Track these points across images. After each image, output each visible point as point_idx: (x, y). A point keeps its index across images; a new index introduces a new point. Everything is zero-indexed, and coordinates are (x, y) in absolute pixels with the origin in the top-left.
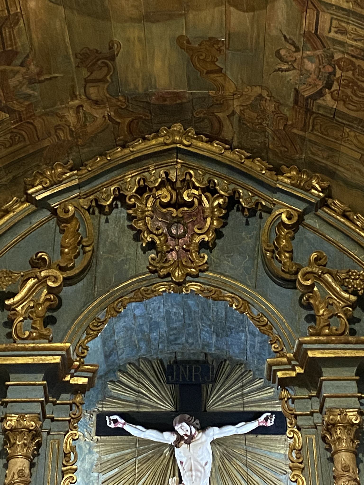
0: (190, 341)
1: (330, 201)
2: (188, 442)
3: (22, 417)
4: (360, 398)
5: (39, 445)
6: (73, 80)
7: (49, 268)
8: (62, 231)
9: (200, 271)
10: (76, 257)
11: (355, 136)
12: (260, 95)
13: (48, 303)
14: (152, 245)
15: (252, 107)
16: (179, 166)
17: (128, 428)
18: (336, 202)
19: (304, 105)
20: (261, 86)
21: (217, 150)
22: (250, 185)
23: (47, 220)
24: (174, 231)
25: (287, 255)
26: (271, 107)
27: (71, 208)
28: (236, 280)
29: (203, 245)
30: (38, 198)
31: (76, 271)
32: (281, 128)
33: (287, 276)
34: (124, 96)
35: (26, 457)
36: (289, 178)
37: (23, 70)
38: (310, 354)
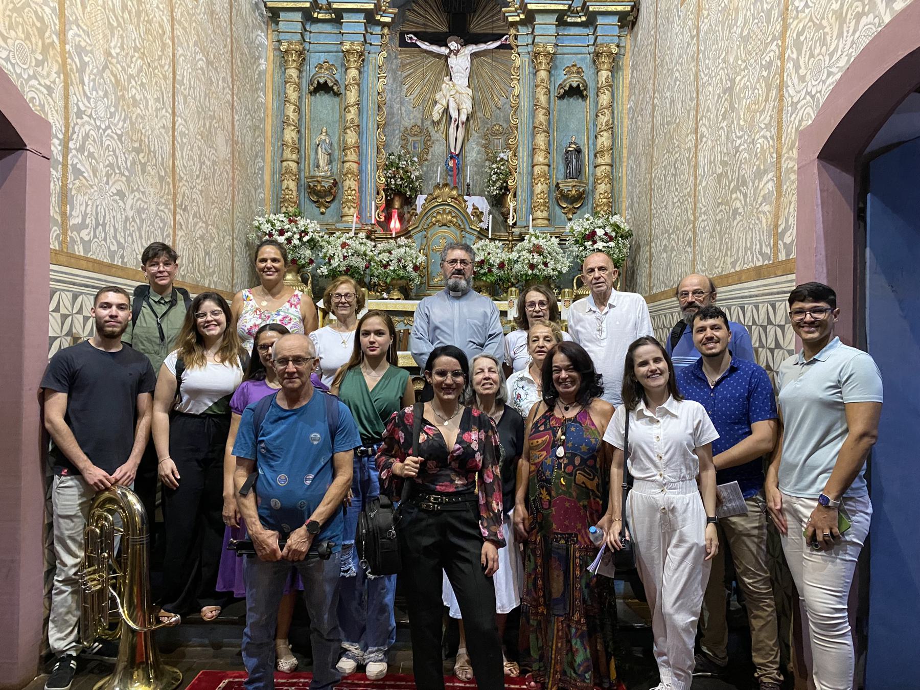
2: (456, 54)
3: (353, 43)
5: (363, 61)
17: (419, 43)
35: (356, 68)
38: (530, 7)
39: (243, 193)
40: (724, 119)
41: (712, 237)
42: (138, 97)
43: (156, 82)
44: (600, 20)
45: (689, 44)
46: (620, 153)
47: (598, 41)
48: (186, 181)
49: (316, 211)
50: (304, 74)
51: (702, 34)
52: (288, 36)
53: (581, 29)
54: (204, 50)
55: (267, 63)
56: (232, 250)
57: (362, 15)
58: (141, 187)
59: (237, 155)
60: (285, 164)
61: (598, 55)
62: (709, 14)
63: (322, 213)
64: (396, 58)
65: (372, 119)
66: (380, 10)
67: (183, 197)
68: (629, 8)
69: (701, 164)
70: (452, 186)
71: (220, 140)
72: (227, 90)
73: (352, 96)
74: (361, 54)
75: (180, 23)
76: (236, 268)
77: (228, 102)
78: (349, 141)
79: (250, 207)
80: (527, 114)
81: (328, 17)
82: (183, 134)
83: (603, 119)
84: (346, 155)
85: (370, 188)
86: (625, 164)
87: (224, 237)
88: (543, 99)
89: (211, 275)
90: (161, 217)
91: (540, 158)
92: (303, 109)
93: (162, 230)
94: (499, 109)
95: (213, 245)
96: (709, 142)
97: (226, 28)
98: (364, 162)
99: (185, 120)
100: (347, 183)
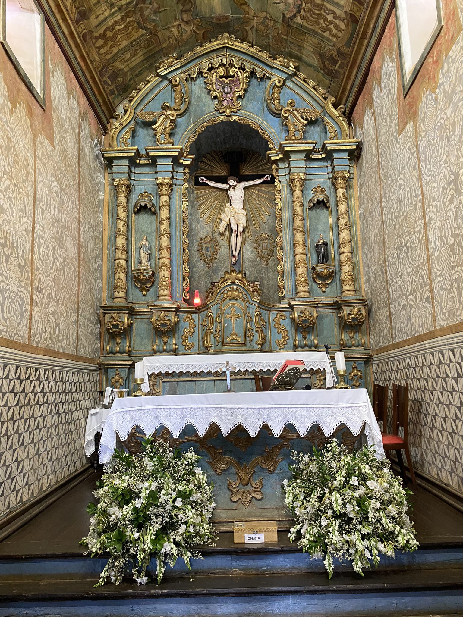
0: (234, 142)
1: (298, 73)
2: (234, 188)
3: (164, 178)
4: (306, 168)
5: (172, 190)
6: (175, 11)
7: (170, 110)
8: (174, 91)
9: (238, 110)
10: (181, 104)
11: (311, 39)
12: (266, 17)
13: (171, 127)
14: (216, 97)
15: (262, 23)
16: (228, 56)
17: (208, 182)
18: (301, 73)
19: (287, 22)
20: (267, 12)
21: (245, 47)
22: (261, 65)
23: (167, 86)
24: (226, 90)
25: (278, 101)
26: (271, 23)
27: (178, 79)
28: (254, 114)
29: (239, 97)
30: (162, 75)
31: (182, 111)
32: (276, 34)
33: (277, 112)
34: (200, 18)
35: (167, 195)
36: (279, 61)
37: (151, 6)
38: (286, 149)
39: (87, 282)
40: (451, 202)
41: (450, 292)
42: (5, 206)
43: (21, 197)
44: (335, 156)
45: (409, 159)
46: (356, 244)
47: (336, 169)
48: (42, 270)
49: (140, 294)
50: (131, 200)
51: (421, 149)
52: (119, 176)
53: (322, 163)
54: (58, 180)
55: (104, 195)
56: (77, 322)
57: (170, 160)
58: (4, 273)
59: (82, 255)
60: (117, 262)
61: (335, 179)
62: (426, 134)
63: (145, 295)
64: (193, 193)
65: (179, 229)
66: (182, 156)
67: (39, 282)
68: (355, 147)
69: (432, 240)
70: (238, 271)
71: (69, 243)
72: (75, 210)
73: (164, 214)
74: (170, 185)
75: (41, 160)
76: (80, 337)
77: (76, 218)
78: (163, 244)
79: (91, 292)
80: (287, 221)
81: (146, 162)
82: (40, 237)
83: (343, 222)
84: (161, 253)
85: (179, 275)
86: (361, 252)
87: (71, 314)
88: (299, 210)
89: (60, 341)
90: (20, 297)
91: (299, 249)
92: (130, 224)
93: (21, 306)
94: (265, 223)
95: (62, 319)
96: (438, 223)
97: (75, 168)
98: (174, 259)
99: (42, 227)
100: (162, 273)
